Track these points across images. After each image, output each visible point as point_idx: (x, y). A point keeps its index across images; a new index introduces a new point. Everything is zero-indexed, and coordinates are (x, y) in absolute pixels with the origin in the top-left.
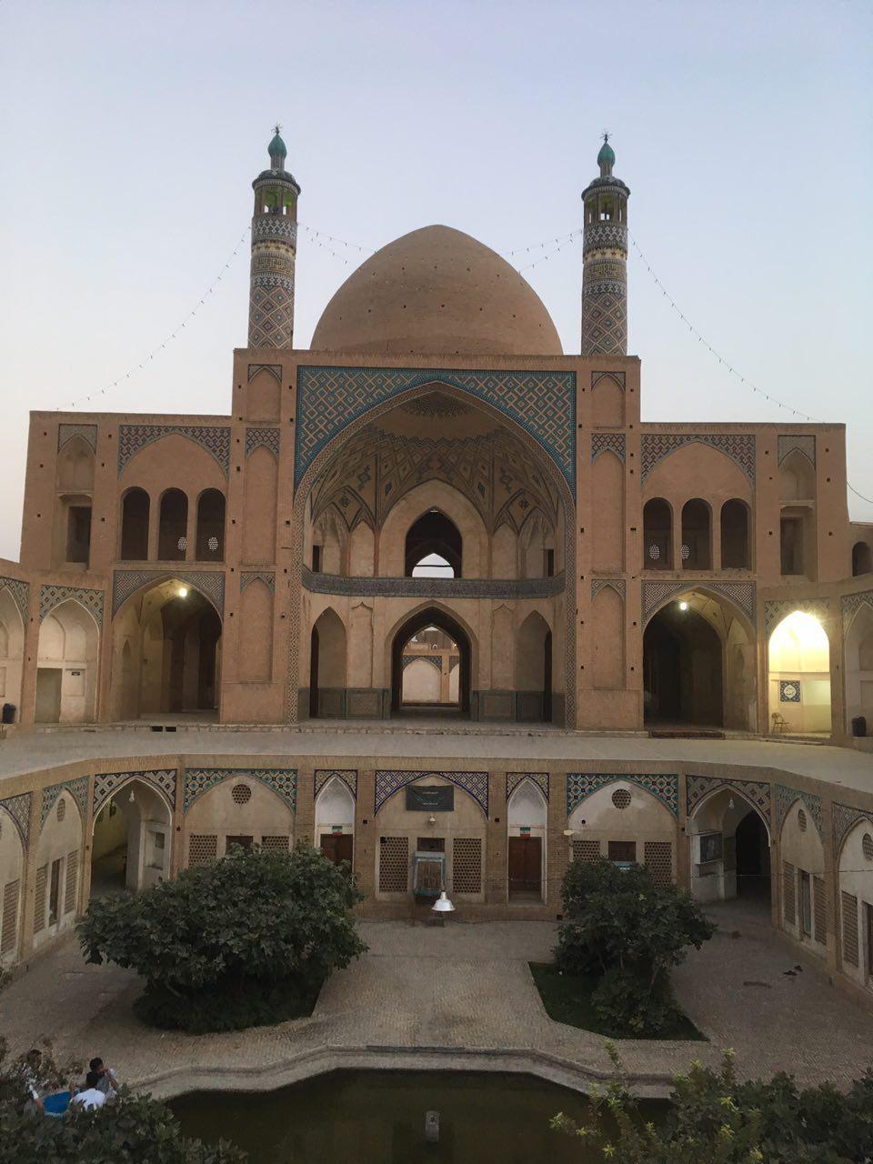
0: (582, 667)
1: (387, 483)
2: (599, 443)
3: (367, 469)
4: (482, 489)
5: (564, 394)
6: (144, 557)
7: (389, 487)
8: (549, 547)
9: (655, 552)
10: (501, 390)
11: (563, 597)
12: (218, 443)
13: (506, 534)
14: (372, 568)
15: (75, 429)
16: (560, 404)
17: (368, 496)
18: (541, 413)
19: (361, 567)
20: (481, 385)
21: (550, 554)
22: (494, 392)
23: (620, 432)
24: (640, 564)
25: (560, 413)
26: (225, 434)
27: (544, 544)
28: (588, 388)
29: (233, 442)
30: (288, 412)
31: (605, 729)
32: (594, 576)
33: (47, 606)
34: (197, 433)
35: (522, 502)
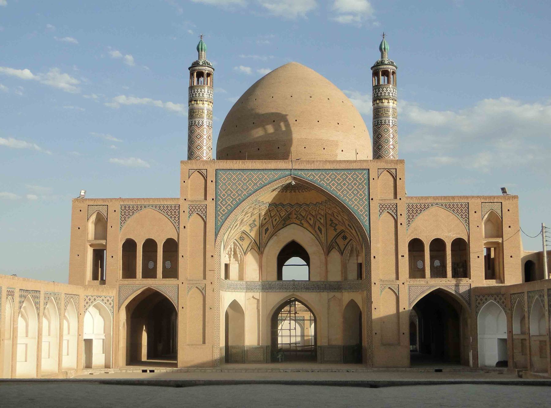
0: (376, 334)
1: (265, 228)
2: (383, 209)
4: (320, 230)
5: (363, 182)
6: (135, 277)
7: (267, 230)
8: (360, 261)
10: (328, 180)
11: (365, 292)
12: (173, 213)
13: (335, 255)
15: (96, 207)
16: (361, 187)
18: (350, 192)
20: (317, 177)
22: (325, 181)
23: (395, 201)
24: (408, 276)
25: (361, 192)
27: (357, 260)
28: (376, 178)
29: (181, 212)
30: (211, 194)
31: (387, 367)
32: (381, 283)
33: (87, 306)
34: (162, 208)
35: (343, 236)
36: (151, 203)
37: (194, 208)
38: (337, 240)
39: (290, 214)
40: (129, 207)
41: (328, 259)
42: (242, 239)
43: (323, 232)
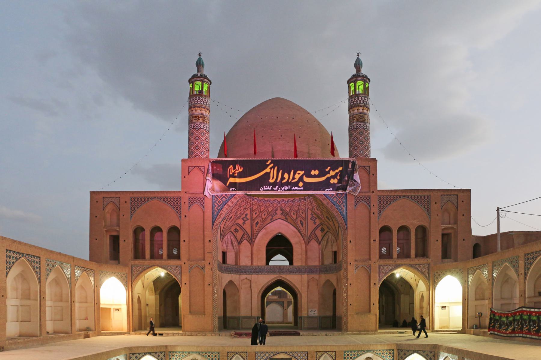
1: (256, 221)
2: (358, 200)
3: (246, 215)
8: (335, 249)
9: (384, 251)
12: (175, 204)
14: (250, 261)
17: (247, 227)
19: (245, 261)
21: (335, 253)
23: (368, 194)
26: (179, 200)
36: (156, 195)
37: (194, 199)
38: (316, 232)
39: (276, 210)
40: (138, 199)
41: (308, 247)
42: (236, 231)
43: (304, 226)
